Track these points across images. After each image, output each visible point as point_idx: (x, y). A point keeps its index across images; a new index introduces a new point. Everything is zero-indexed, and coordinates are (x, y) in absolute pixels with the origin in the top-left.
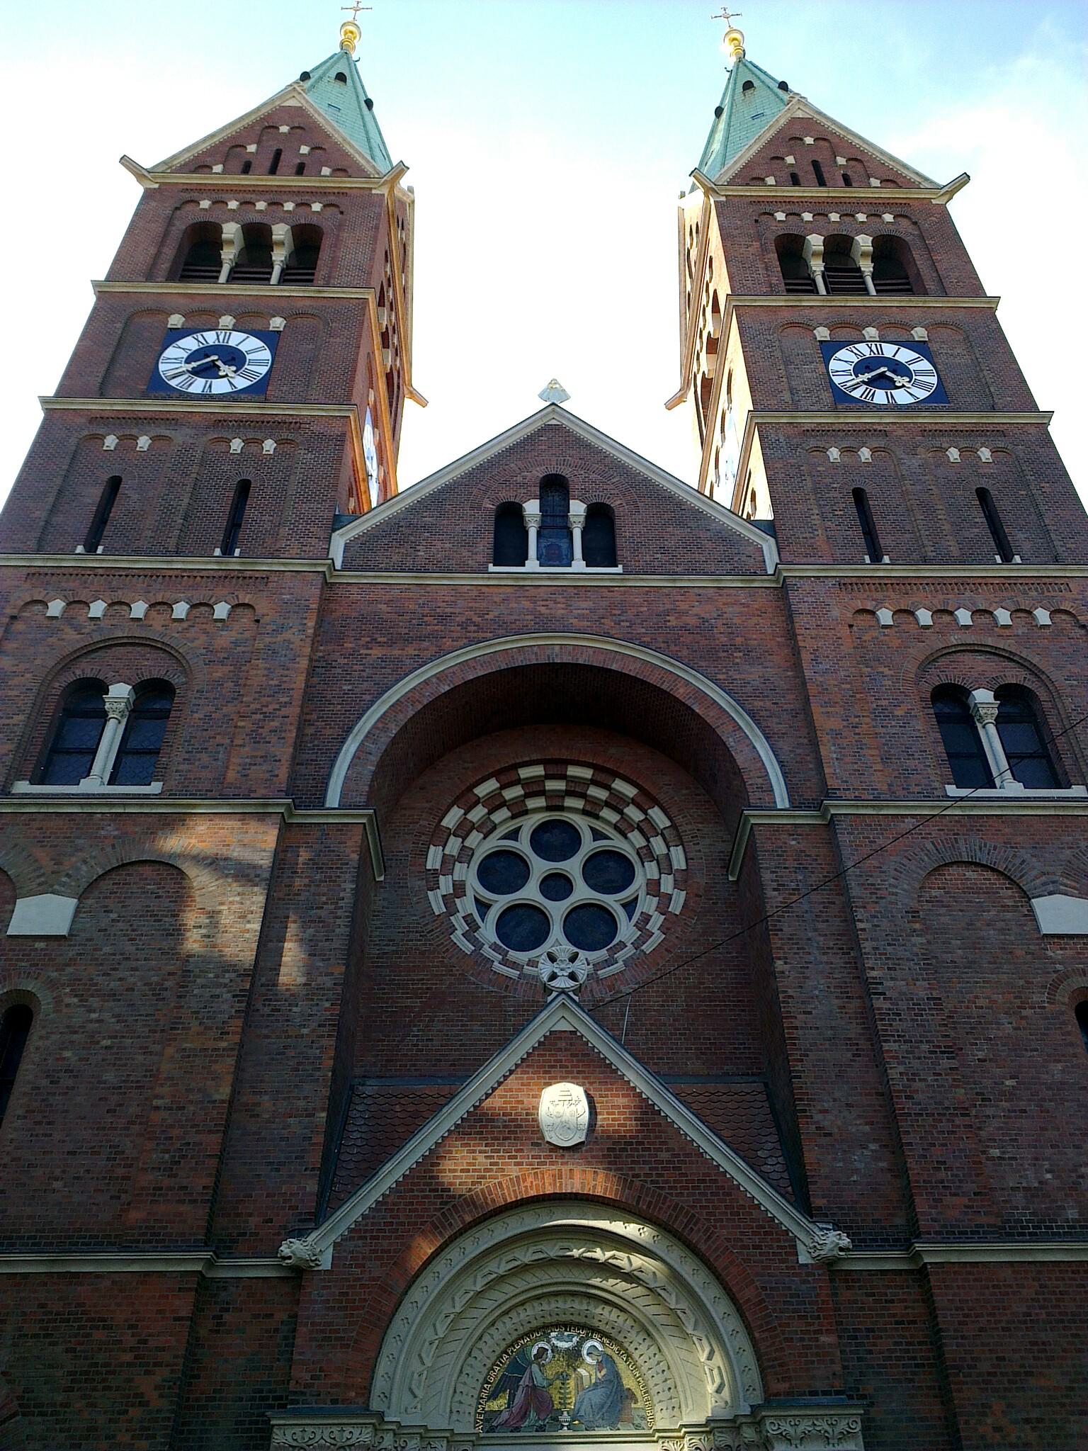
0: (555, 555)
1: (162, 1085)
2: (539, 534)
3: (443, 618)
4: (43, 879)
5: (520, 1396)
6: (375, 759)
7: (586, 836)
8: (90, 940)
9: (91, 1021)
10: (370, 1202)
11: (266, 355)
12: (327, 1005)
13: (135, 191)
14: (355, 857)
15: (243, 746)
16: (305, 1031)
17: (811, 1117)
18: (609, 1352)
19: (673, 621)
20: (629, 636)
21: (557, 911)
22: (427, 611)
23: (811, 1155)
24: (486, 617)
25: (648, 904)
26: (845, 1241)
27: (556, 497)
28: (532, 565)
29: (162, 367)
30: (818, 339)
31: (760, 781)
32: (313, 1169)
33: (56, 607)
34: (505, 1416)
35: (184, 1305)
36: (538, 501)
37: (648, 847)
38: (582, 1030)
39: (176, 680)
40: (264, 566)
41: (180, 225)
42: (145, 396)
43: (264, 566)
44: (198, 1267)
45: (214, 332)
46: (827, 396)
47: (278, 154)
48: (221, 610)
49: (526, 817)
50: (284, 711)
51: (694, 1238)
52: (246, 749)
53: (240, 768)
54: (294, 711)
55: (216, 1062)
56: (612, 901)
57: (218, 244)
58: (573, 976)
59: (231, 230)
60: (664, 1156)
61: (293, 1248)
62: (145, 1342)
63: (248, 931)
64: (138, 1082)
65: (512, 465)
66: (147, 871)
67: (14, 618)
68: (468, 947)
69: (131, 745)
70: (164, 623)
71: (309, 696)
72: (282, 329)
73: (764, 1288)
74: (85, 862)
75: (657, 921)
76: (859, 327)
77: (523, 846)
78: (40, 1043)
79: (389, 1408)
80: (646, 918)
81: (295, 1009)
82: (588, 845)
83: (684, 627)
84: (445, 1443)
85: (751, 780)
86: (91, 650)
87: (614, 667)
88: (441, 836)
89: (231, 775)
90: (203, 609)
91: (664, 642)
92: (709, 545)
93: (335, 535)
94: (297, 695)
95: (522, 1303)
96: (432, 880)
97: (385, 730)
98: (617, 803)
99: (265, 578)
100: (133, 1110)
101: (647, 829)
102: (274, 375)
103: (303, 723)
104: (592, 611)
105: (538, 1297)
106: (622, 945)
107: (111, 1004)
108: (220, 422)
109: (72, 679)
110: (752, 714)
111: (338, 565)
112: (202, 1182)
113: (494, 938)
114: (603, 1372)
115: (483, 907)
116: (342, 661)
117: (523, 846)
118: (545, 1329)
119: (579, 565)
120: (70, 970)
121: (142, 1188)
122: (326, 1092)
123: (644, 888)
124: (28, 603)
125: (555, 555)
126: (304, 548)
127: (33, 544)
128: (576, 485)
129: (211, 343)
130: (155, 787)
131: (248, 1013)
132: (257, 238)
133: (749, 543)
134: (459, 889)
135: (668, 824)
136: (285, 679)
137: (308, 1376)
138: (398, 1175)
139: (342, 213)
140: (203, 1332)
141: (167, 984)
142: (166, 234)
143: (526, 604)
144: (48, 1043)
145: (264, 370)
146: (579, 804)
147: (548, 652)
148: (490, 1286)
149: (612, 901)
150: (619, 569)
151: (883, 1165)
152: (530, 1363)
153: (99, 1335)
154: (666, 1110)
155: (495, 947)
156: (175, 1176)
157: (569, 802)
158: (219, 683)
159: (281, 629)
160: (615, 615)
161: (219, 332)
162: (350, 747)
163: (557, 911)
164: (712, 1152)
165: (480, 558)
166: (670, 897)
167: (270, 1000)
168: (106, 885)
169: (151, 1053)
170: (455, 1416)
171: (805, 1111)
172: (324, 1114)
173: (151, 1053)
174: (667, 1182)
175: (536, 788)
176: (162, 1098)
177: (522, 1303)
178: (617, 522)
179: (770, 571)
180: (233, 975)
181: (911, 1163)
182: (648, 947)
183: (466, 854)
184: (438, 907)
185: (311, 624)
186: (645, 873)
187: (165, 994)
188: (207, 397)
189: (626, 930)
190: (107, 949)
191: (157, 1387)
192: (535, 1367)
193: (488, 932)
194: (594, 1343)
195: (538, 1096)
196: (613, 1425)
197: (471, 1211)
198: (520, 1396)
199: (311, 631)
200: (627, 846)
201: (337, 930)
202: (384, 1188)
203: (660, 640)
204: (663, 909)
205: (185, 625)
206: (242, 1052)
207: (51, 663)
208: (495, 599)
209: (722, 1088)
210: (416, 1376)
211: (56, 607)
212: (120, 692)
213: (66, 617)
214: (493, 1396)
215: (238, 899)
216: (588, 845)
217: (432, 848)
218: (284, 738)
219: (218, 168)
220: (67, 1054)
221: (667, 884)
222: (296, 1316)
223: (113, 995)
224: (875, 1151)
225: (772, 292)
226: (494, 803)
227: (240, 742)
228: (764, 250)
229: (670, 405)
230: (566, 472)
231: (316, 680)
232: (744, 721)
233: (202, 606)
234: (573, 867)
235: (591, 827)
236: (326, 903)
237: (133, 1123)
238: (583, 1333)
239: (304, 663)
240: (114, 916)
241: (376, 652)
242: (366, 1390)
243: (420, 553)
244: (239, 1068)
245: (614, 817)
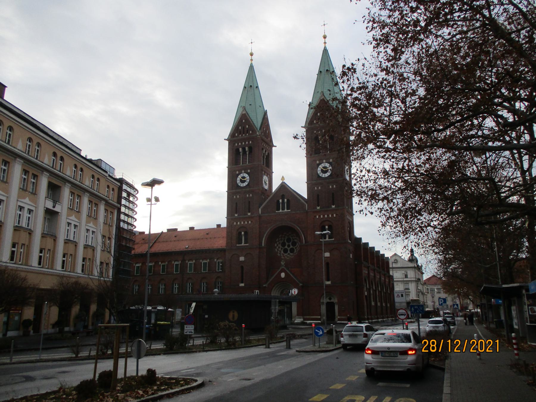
13: (227, 142)
21: (289, 249)
28: (281, 211)
47: (244, 127)
48: (250, 222)
119: (286, 210)
125: (283, 209)
162: (264, 239)
163: (289, 249)
200: (296, 241)
211: (235, 223)
219: (236, 135)
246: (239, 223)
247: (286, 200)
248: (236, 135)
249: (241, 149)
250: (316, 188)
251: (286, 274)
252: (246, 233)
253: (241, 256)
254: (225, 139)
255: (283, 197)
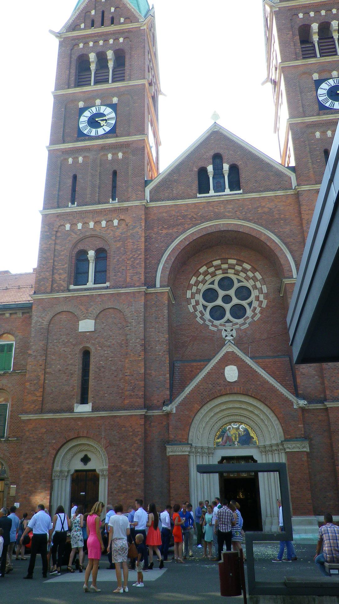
0: (219, 188)
1: (126, 370)
2: (213, 178)
3: (184, 217)
4: (84, 315)
5: (225, 439)
6: (168, 269)
7: (236, 281)
8: (100, 332)
9: (106, 354)
10: (183, 397)
11: (113, 115)
12: (165, 346)
14: (166, 302)
15: (130, 269)
16: (160, 353)
17: (299, 370)
18: (246, 428)
19: (260, 210)
20: (245, 218)
21: (228, 307)
22: (178, 214)
23: (298, 380)
24: (198, 215)
25: (255, 304)
26: (306, 402)
27: (218, 161)
28: (212, 192)
29: (81, 126)
30: (314, 79)
31: (288, 268)
32: (168, 389)
33: (68, 227)
34: (221, 443)
35: (142, 422)
36: (212, 166)
37: (255, 285)
38: (235, 351)
39: (106, 248)
40: (126, 204)
41: (75, 57)
42: (77, 141)
43: (126, 204)
44: (144, 413)
45: (95, 107)
46: (316, 107)
47: (103, 13)
48: (116, 222)
49: (216, 277)
50: (140, 257)
51: (266, 403)
52: (131, 271)
53: (130, 277)
54: (142, 256)
55: (139, 363)
56: (244, 303)
57: (89, 63)
58: (232, 336)
59: (92, 57)
60: (259, 383)
61: (166, 409)
62: (134, 430)
63: (141, 327)
64: (120, 369)
65: (202, 151)
66: (110, 310)
67: (57, 232)
68: (201, 322)
69: (97, 270)
70: (100, 228)
71: (146, 250)
72: (117, 102)
73: (284, 414)
74: (94, 309)
75: (258, 310)
76: (330, 71)
77: (216, 286)
78: (94, 360)
79: (193, 442)
80: (255, 309)
81: (157, 348)
82: (236, 285)
83: (264, 213)
84: (207, 449)
85: (286, 268)
86: (81, 240)
87: (241, 230)
88: (190, 287)
89: (128, 280)
90: (110, 222)
91: (257, 219)
92: (272, 178)
93: (146, 188)
94: (143, 250)
95: (224, 418)
96: (188, 301)
97: (170, 259)
98: (245, 271)
99: (127, 209)
100: (121, 376)
101: (255, 279)
102: (118, 124)
103: (146, 259)
104: (233, 209)
105: (228, 416)
106: (248, 318)
107: (109, 349)
108: (105, 148)
109: (77, 250)
110: (286, 244)
111: (148, 201)
112: (141, 393)
113: (209, 317)
114: (245, 432)
115: (205, 307)
116: (154, 236)
117: (216, 286)
118: (230, 423)
119: (227, 191)
120: (97, 340)
121: (127, 395)
122: (168, 369)
123: (254, 298)
124: (59, 226)
125: (219, 188)
126: (137, 196)
127: (56, 204)
128: (225, 158)
129: (95, 113)
130: (108, 284)
131: (145, 350)
132: (102, 59)
133: (286, 176)
134: (197, 303)
135: (261, 278)
136: (139, 245)
137: (173, 437)
138: (189, 390)
139: (131, 41)
140: (147, 427)
141: (123, 343)
142: (70, 62)
143: (211, 208)
144: (96, 360)
145: (113, 122)
146: (233, 271)
147: (219, 227)
148: (215, 414)
149: (244, 303)
150: (241, 191)
151: (319, 382)
152: (226, 431)
153: (123, 429)
154: (259, 371)
155: (210, 321)
156: (134, 392)
157: (230, 271)
158: (119, 248)
159: (134, 227)
160: (240, 210)
161: (96, 107)
164: (271, 381)
165: (194, 192)
166: (262, 302)
167: (150, 345)
168: (101, 315)
169: (122, 361)
170: (209, 444)
171: (298, 368)
172: (168, 375)
173: (122, 361)
174: (259, 389)
175: (218, 268)
176: (127, 373)
177: (224, 418)
178: (240, 171)
179: (294, 188)
180: (139, 340)
181: (326, 382)
182: (256, 319)
183: (198, 291)
184: (192, 310)
185: (143, 224)
186: (255, 293)
187: (123, 346)
188: (98, 137)
189: (249, 313)
190: (105, 334)
191: (139, 440)
192: (228, 432)
193: (207, 316)
194: (243, 426)
195: (224, 369)
196: (248, 445)
197: (209, 398)
198: (225, 439)
199: (143, 227)
200: (249, 284)
201: (165, 325)
202: (186, 393)
203: (256, 218)
204: (260, 306)
205: (106, 229)
206: (145, 360)
207: (71, 246)
208: (201, 208)
209: (277, 359)
210: (199, 435)
211: (68, 227)
212: (91, 254)
213: (72, 230)
214: (218, 438)
215: (137, 318)
216: (236, 285)
217: (188, 291)
218: (141, 266)
219: (82, 26)
220: (101, 363)
221: (261, 297)
222: (168, 423)
223: (109, 346)
224: (317, 378)
225: (296, 59)
226: (206, 273)
227: (129, 268)
228: (294, 35)
229: (264, 83)
230: (221, 152)
231: (147, 243)
232: (283, 247)
233: (109, 221)
234: (232, 293)
235: (237, 279)
236: (160, 317)
237: (121, 379)
238: (240, 424)
239: (143, 239)
240: (105, 324)
241: (164, 232)
242: (188, 439)
243: (174, 192)
244: (145, 364)
245: (244, 275)
246: (80, 226)
247: (226, 167)
248: (82, 26)
249: (92, 57)
250: (318, 134)
251: (243, 369)
252: (101, 254)
253: (86, 318)
254: (51, 32)
255: (217, 159)
